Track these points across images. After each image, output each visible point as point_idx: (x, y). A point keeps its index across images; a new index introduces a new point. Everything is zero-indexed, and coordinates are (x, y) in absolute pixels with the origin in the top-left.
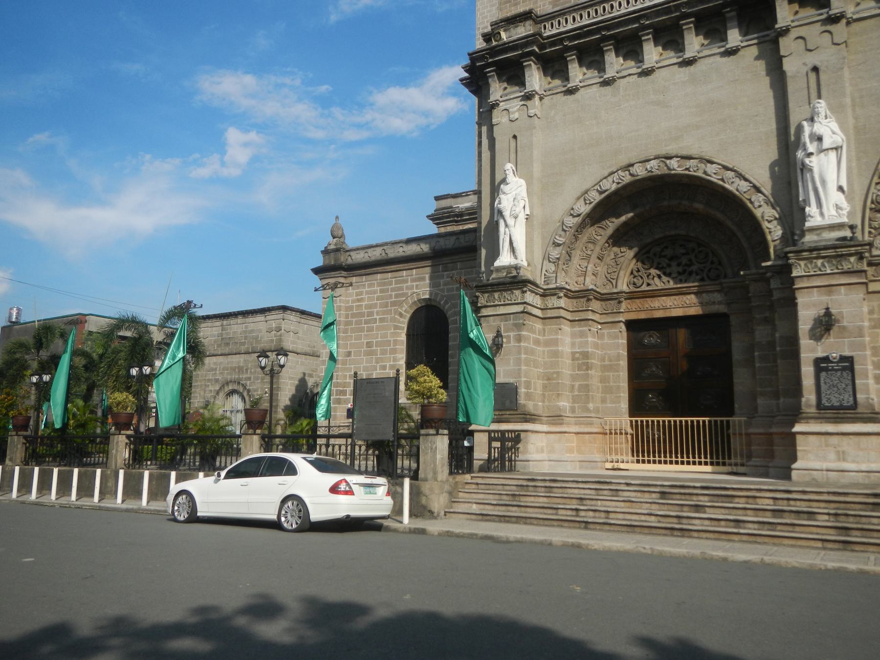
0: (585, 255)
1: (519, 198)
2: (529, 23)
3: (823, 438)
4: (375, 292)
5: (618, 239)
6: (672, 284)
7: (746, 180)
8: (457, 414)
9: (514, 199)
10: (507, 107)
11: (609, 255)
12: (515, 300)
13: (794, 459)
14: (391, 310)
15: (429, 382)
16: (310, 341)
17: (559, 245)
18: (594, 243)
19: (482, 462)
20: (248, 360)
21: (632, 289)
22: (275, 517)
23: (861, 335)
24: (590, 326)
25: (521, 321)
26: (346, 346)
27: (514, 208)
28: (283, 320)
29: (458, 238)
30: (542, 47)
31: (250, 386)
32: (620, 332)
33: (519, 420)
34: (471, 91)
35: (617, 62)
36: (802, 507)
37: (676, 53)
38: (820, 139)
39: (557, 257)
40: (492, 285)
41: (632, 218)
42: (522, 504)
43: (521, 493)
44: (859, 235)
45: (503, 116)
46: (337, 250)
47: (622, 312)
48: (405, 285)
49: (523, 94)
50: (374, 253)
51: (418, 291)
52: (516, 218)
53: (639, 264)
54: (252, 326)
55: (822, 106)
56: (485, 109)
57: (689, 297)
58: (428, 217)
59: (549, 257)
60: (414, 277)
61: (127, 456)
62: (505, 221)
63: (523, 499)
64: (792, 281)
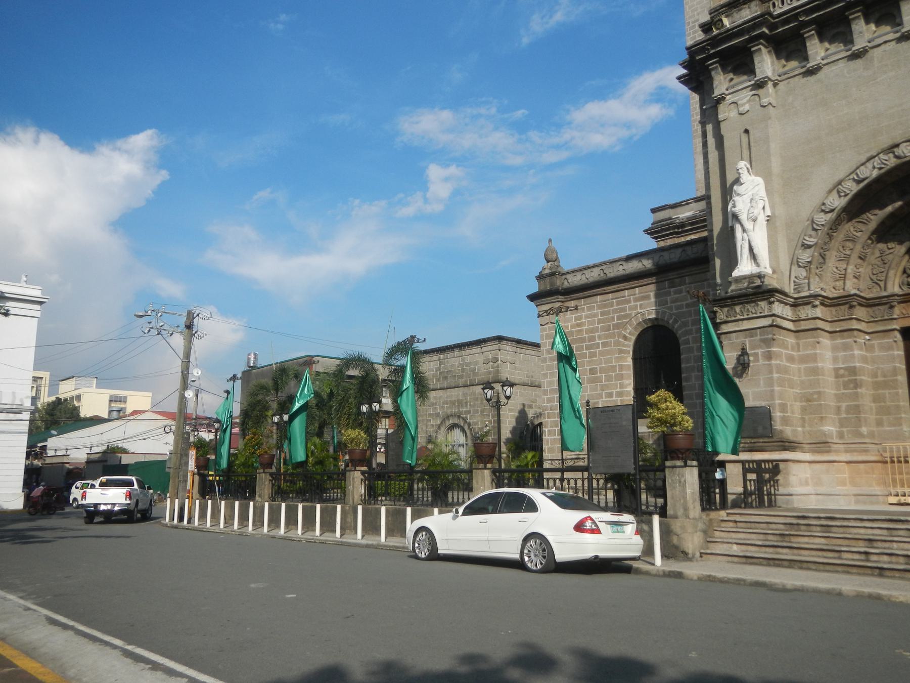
0: (843, 255)
1: (757, 198)
4: (595, 315)
5: (883, 234)
8: (705, 443)
9: (752, 200)
11: (873, 253)
12: (761, 313)
14: (614, 333)
15: (672, 409)
16: (528, 371)
17: (809, 247)
18: (853, 240)
19: (734, 497)
20: (467, 394)
22: (517, 556)
24: (855, 337)
25: (770, 336)
27: (752, 210)
28: (500, 350)
29: (684, 250)
30: (772, 27)
31: (470, 419)
32: (895, 341)
33: (776, 448)
34: (690, 89)
35: (867, 30)
39: (809, 260)
40: (732, 298)
41: (901, 207)
42: (795, 545)
43: (792, 533)
45: (730, 111)
46: (552, 274)
47: (895, 319)
48: (627, 306)
49: (753, 82)
50: (592, 274)
51: (642, 311)
52: (755, 220)
54: (468, 359)
56: (709, 106)
58: (645, 231)
59: (798, 262)
60: (637, 296)
61: (363, 492)
62: (742, 226)
63: (794, 539)
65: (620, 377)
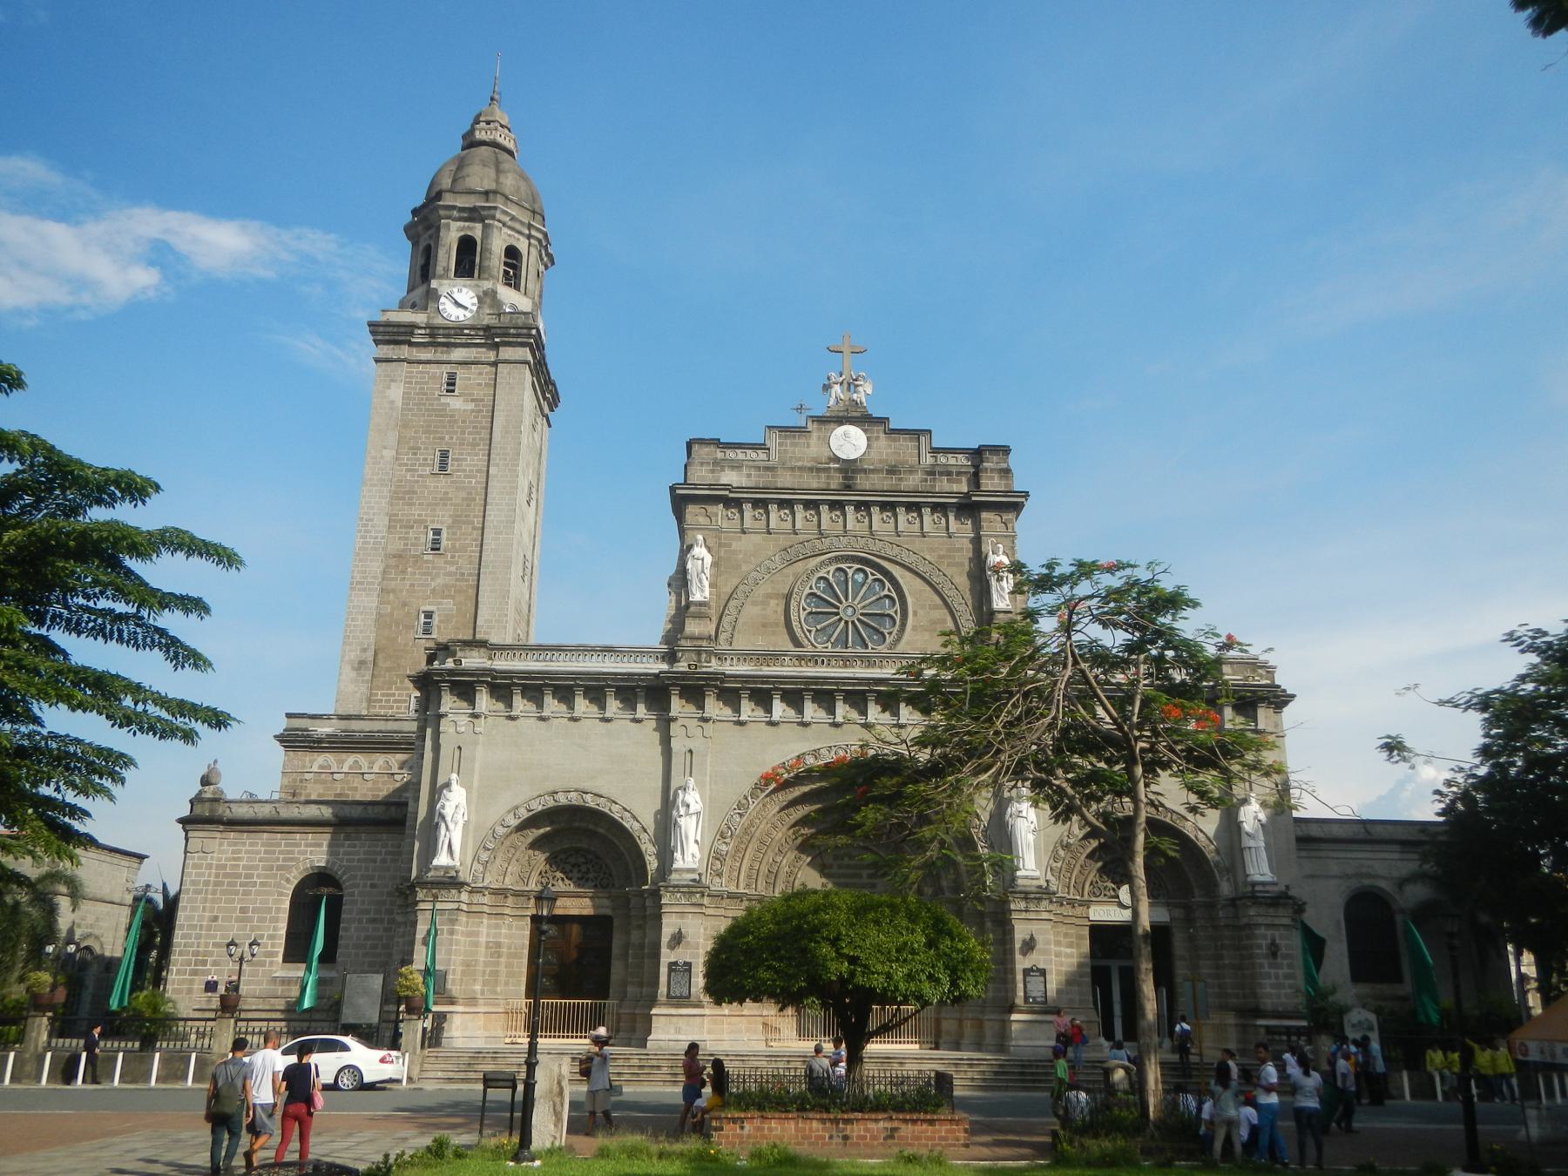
1: (461, 806)
2: (482, 650)
3: (668, 1018)
4: (258, 852)
5: (534, 845)
6: (572, 888)
7: (638, 821)
10: (455, 719)
13: (649, 1032)
17: (489, 850)
23: (698, 949)
26: (212, 909)
30: (494, 678)
36: (655, 1063)
38: (688, 806)
40: (432, 883)
44: (704, 881)
46: (215, 800)
49: (471, 711)
58: (275, 737)
63: (476, 1066)
64: (660, 907)
65: (276, 920)
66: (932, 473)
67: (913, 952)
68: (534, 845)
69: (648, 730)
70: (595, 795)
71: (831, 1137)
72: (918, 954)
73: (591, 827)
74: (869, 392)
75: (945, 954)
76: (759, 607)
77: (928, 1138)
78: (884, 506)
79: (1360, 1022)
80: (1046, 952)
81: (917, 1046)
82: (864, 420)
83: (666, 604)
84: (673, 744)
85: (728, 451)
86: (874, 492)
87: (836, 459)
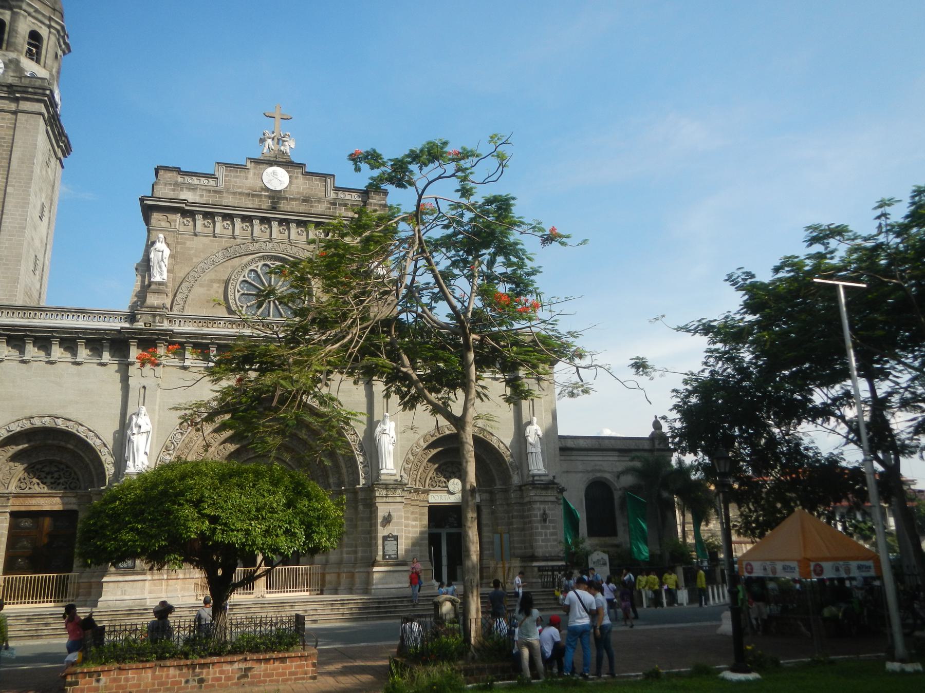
3: (116, 584)
5: (14, 458)
6: (46, 490)
13: (100, 596)
21: (19, 491)
37: (72, 355)
38: (140, 427)
53: (26, 474)
55: (143, 410)
57: (55, 499)
66: (334, 204)
67: (273, 511)
68: (14, 458)
69: (111, 372)
70: (65, 419)
71: (187, 682)
72: (276, 513)
73: (63, 444)
74: (293, 146)
75: (302, 512)
76: (205, 288)
77: (278, 675)
78: (300, 223)
79: (598, 560)
80: (399, 524)
81: (308, 593)
82: (288, 164)
83: (134, 284)
84: (130, 382)
85: (186, 178)
86: (292, 213)
87: (267, 189)
